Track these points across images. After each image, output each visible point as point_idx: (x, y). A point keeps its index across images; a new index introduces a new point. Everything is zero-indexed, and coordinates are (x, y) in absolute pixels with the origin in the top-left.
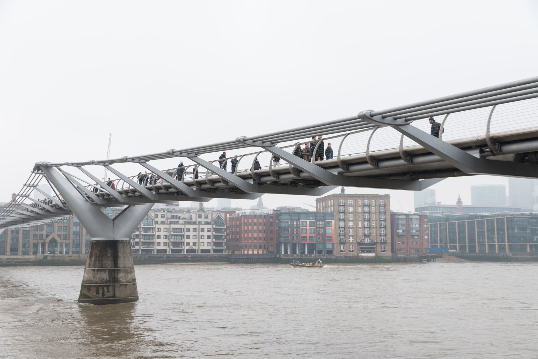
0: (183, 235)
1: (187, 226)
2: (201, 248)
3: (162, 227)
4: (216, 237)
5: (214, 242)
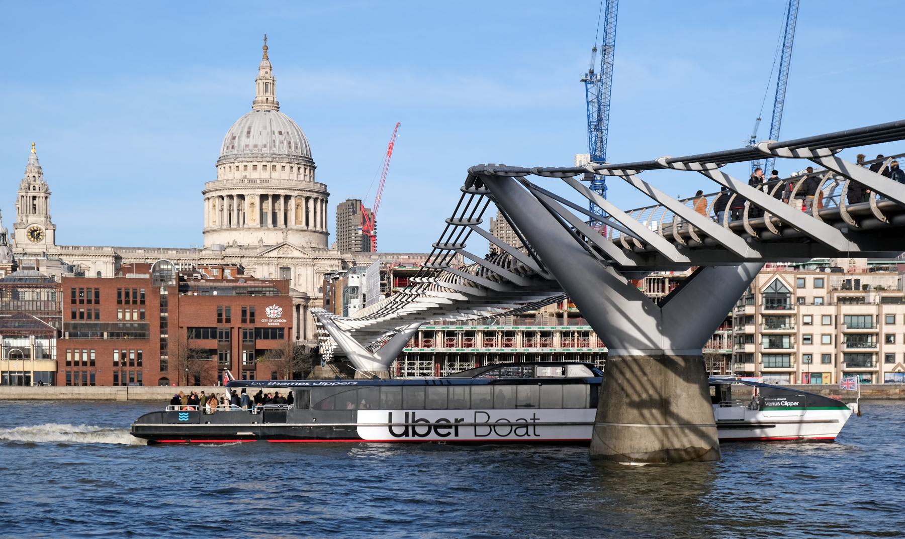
1: (888, 309)
3: (817, 311)
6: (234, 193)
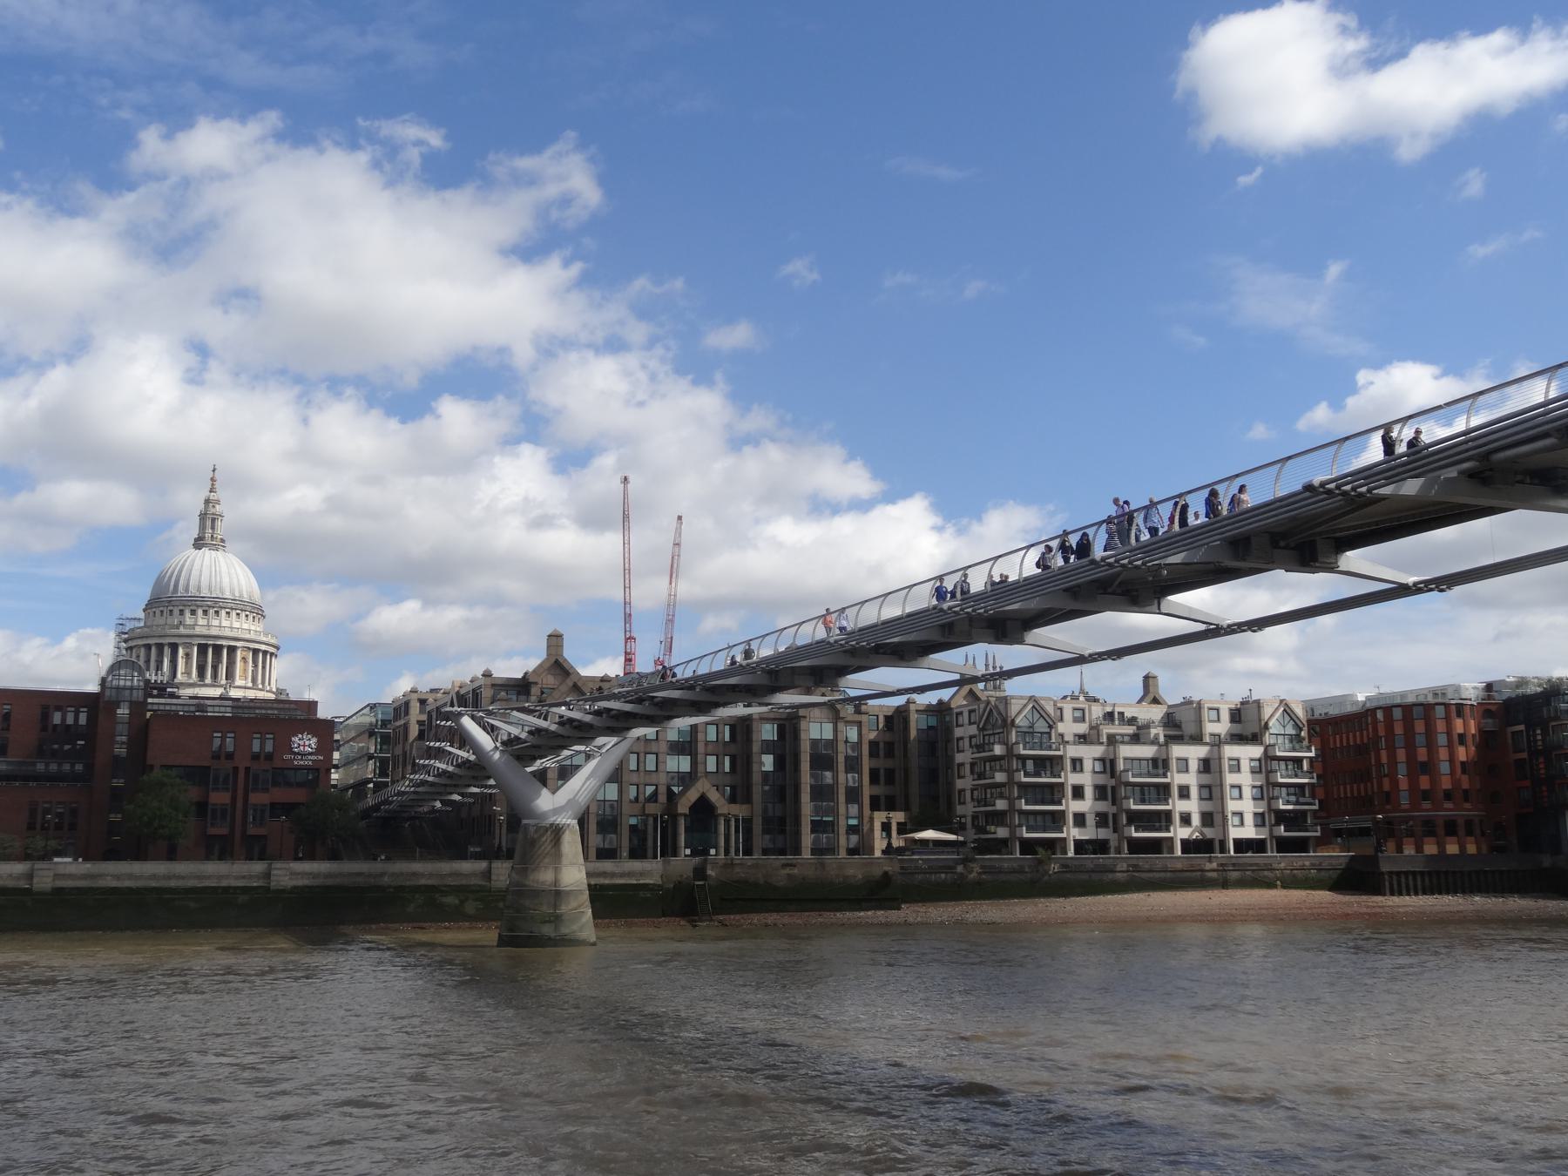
1: (1178, 751)
2: (1235, 833)
3: (1090, 753)
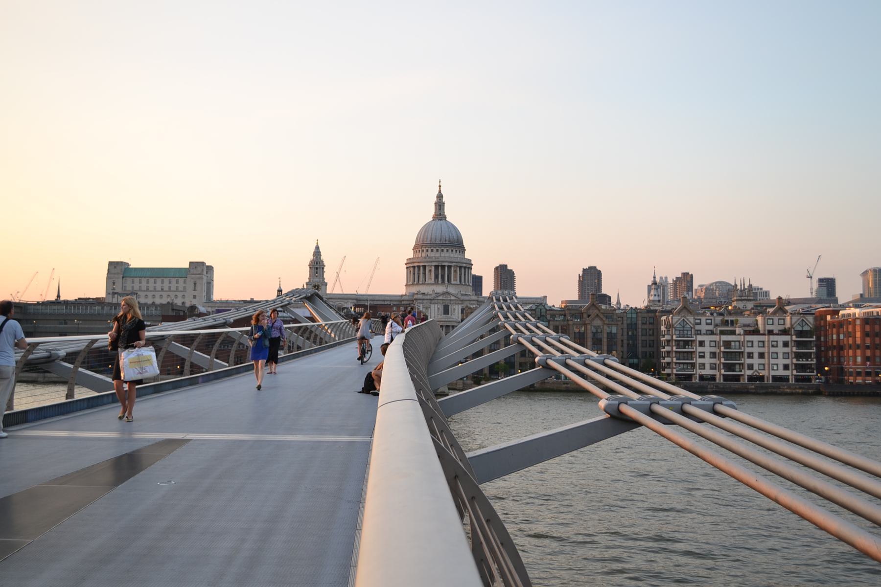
0: (742, 353)
1: (749, 338)
2: (773, 373)
3: (707, 339)
4: (798, 356)
5: (796, 365)
6: (421, 264)
